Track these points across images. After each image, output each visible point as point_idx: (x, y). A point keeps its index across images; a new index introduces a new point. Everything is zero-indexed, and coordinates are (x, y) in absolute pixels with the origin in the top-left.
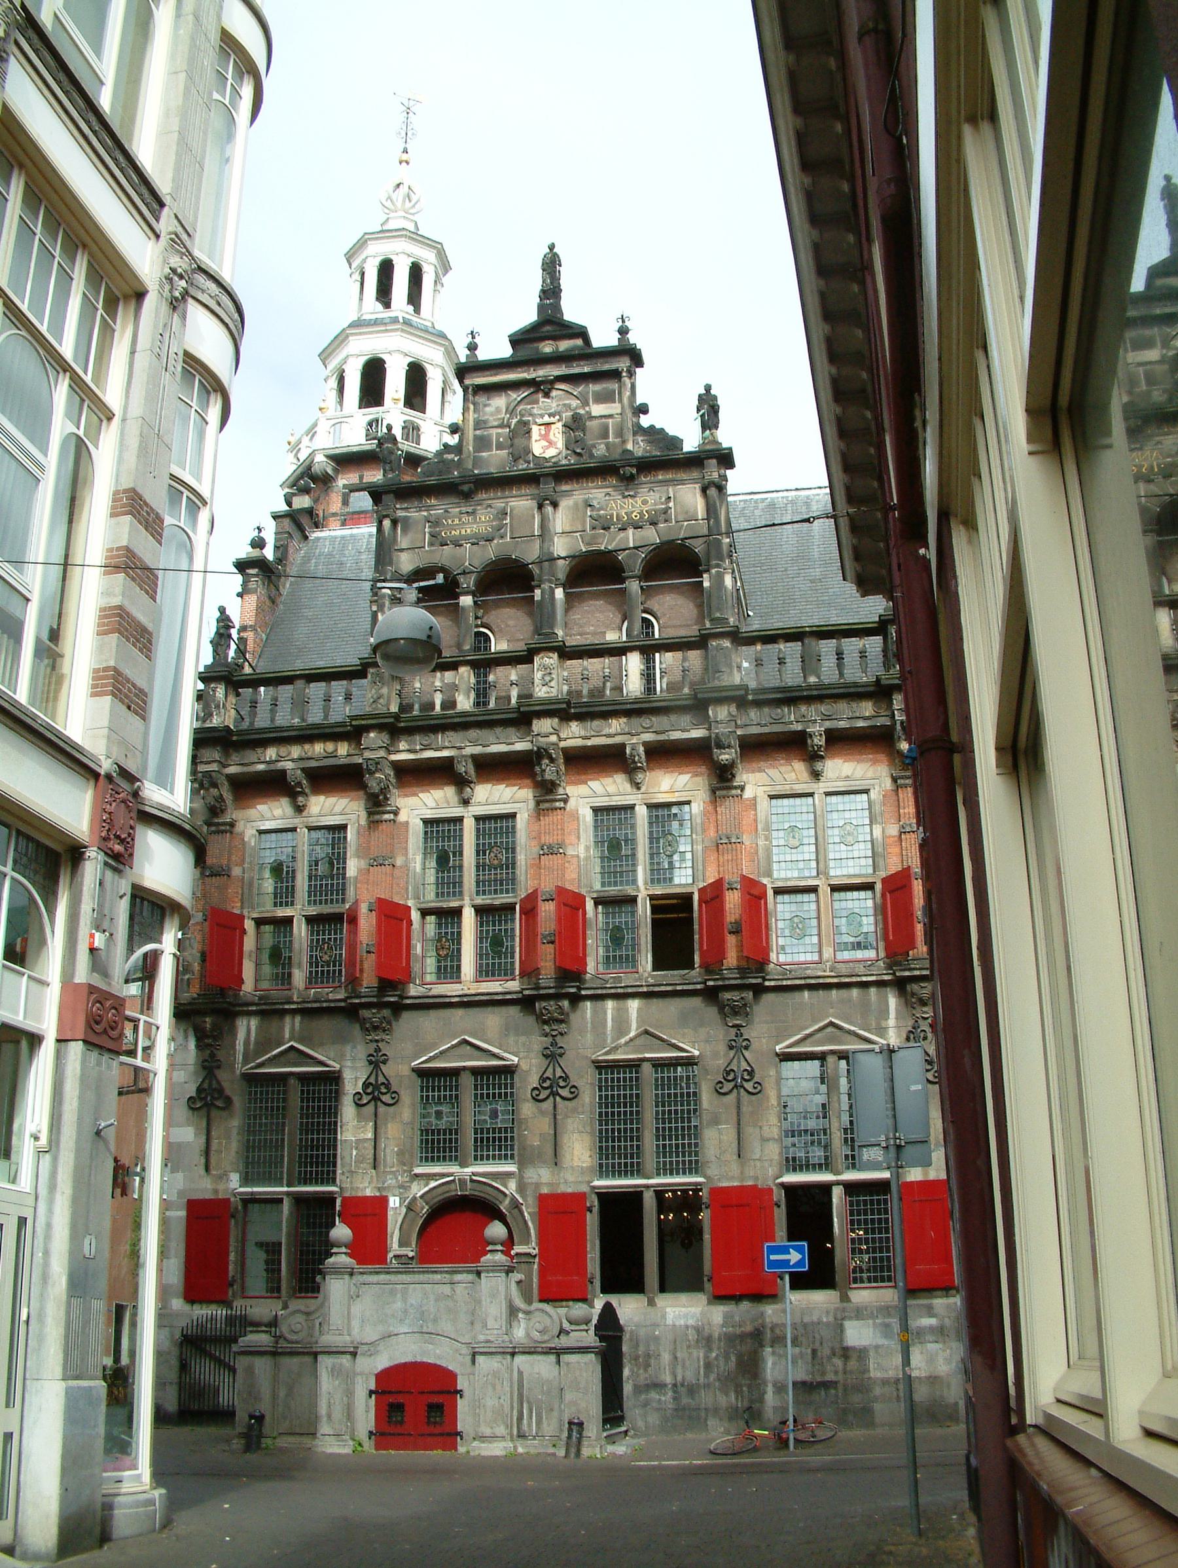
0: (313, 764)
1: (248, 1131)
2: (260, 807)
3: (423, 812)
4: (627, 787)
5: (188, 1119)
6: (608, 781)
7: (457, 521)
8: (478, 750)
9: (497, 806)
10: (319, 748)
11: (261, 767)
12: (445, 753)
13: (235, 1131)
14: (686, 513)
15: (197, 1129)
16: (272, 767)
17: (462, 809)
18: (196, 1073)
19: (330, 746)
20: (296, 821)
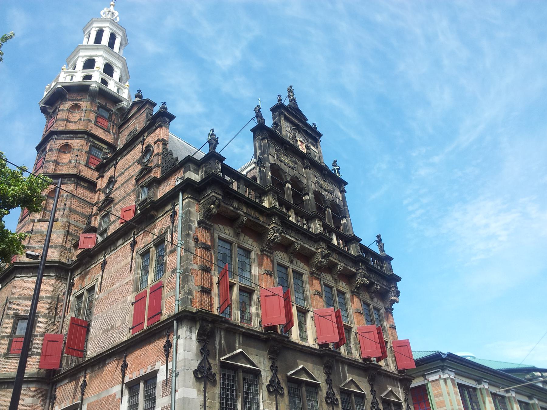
0: (251, 218)
1: (221, 397)
2: (220, 226)
3: (278, 258)
4: (331, 279)
5: (193, 384)
6: (327, 275)
7: (283, 155)
8: (302, 243)
9: (298, 268)
10: (253, 213)
11: (232, 208)
12: (293, 239)
13: (217, 396)
14: (338, 196)
15: (198, 391)
16: (236, 211)
17: (290, 264)
18: (197, 354)
19: (257, 215)
20: (234, 239)
